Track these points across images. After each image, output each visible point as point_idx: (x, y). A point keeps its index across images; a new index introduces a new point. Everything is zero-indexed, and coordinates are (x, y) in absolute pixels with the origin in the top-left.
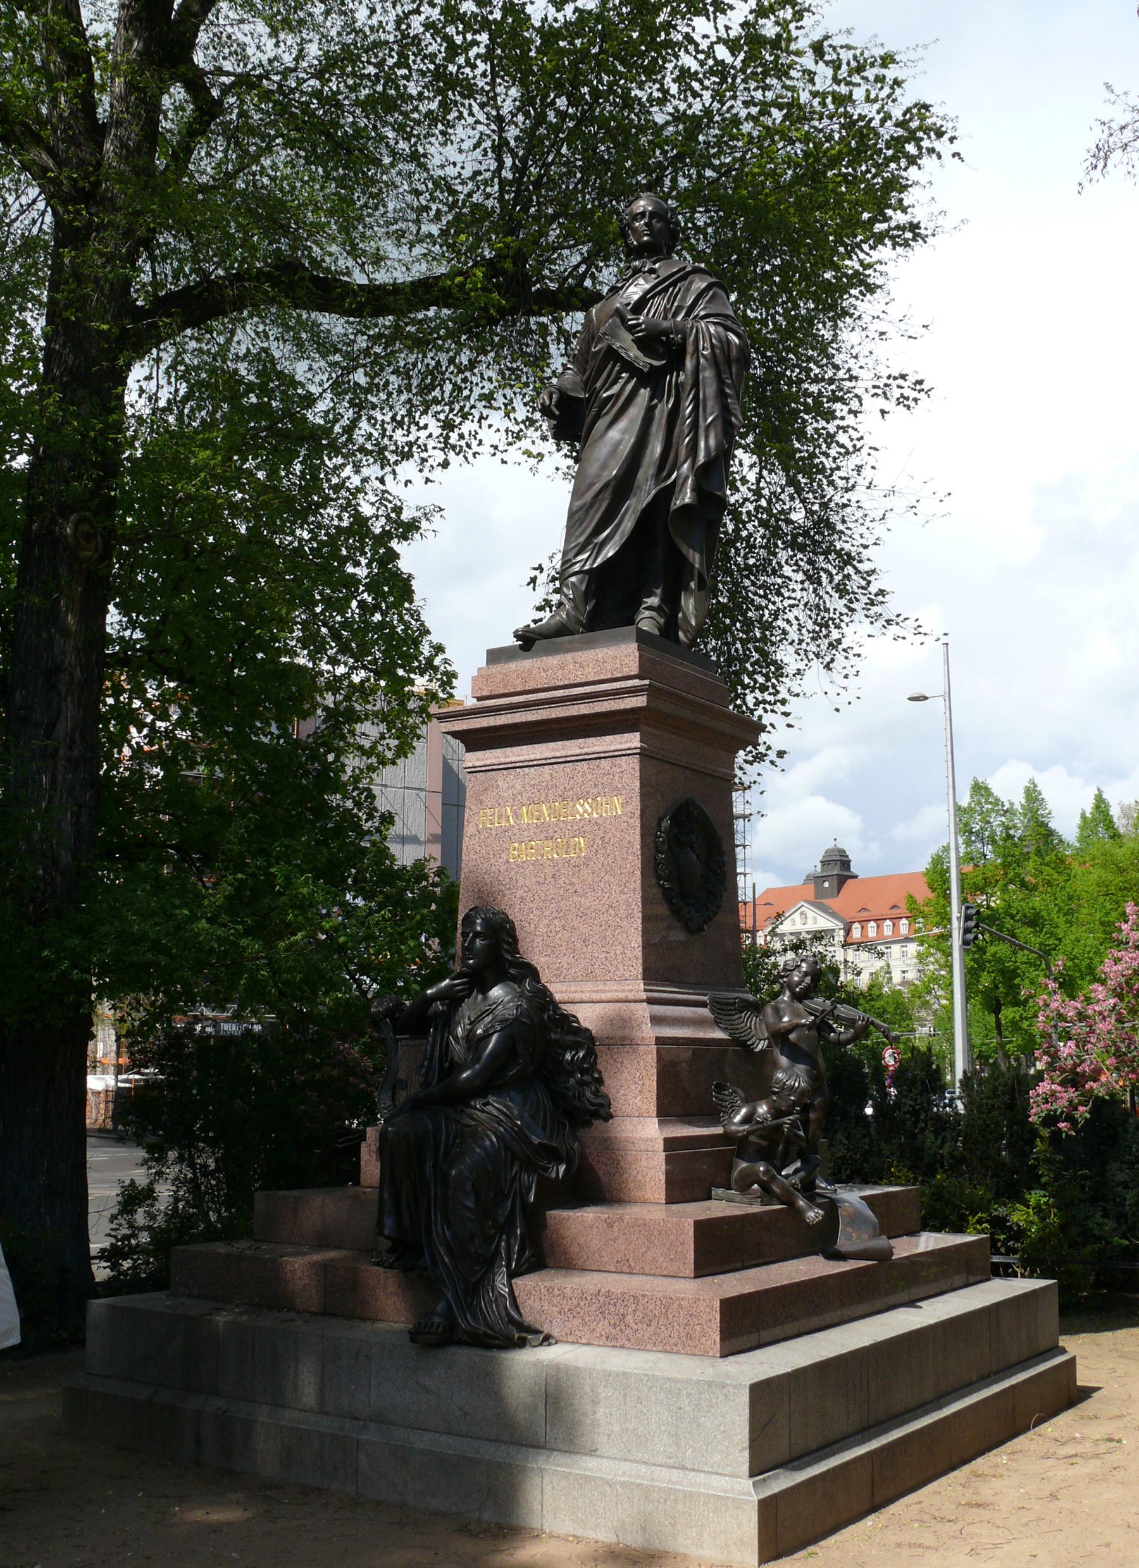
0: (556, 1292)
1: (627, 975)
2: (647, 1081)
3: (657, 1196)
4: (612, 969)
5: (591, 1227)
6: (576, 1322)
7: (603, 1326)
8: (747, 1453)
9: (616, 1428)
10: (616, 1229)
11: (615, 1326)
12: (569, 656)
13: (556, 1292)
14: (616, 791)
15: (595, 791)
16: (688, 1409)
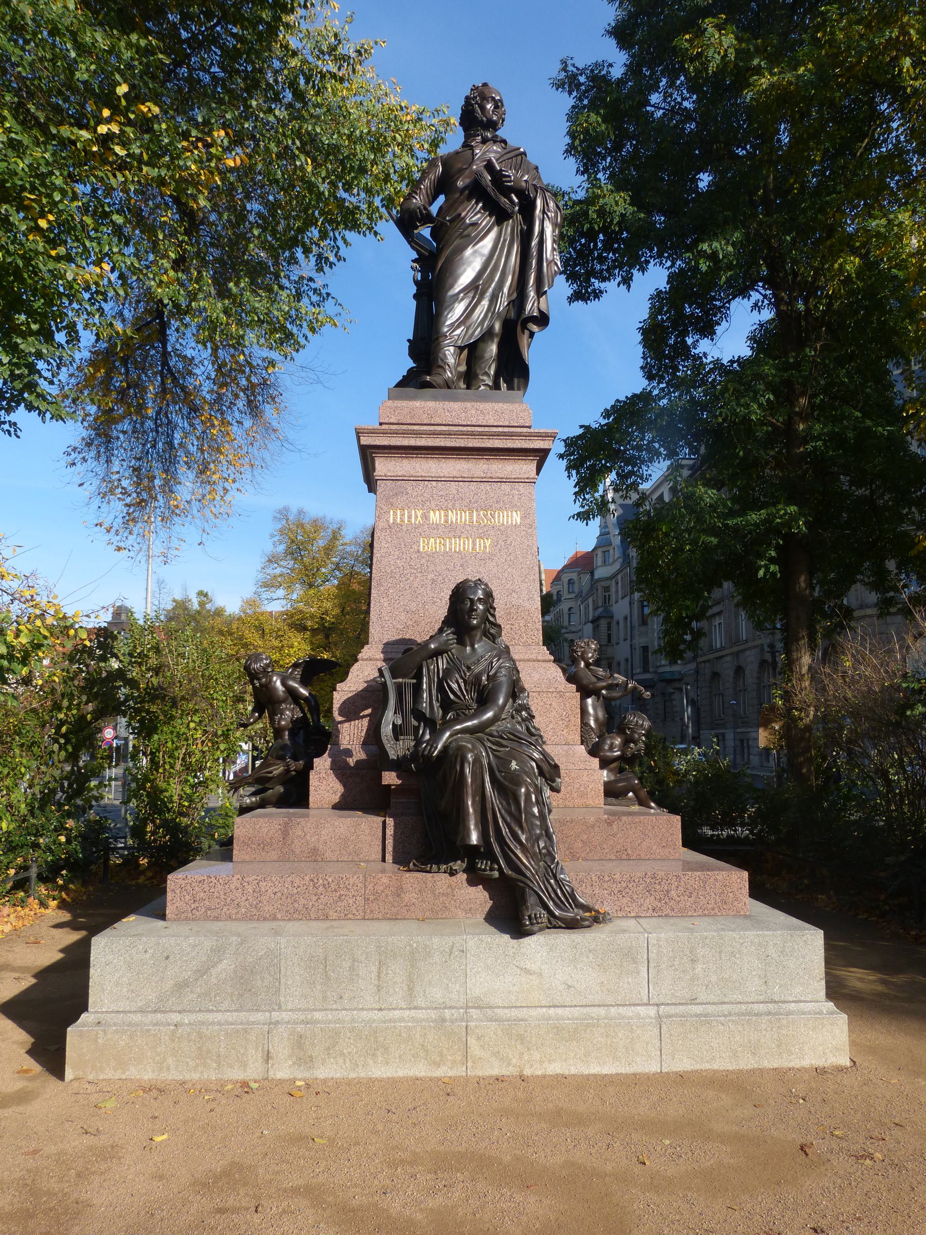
0: (607, 878)
1: (530, 641)
2: (572, 719)
3: (597, 801)
4: (517, 637)
5: (593, 827)
6: (625, 901)
7: (650, 901)
8: (823, 983)
9: (714, 979)
10: (615, 827)
11: (660, 900)
12: (469, 405)
13: (607, 878)
14: (514, 507)
15: (498, 506)
16: (775, 955)
